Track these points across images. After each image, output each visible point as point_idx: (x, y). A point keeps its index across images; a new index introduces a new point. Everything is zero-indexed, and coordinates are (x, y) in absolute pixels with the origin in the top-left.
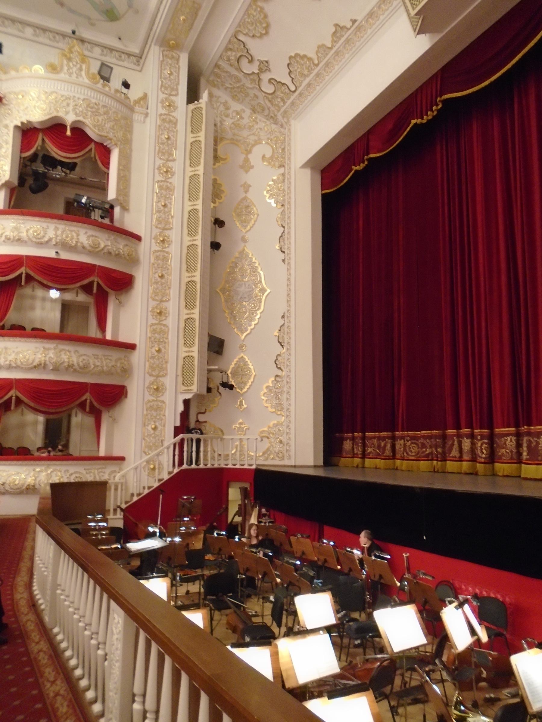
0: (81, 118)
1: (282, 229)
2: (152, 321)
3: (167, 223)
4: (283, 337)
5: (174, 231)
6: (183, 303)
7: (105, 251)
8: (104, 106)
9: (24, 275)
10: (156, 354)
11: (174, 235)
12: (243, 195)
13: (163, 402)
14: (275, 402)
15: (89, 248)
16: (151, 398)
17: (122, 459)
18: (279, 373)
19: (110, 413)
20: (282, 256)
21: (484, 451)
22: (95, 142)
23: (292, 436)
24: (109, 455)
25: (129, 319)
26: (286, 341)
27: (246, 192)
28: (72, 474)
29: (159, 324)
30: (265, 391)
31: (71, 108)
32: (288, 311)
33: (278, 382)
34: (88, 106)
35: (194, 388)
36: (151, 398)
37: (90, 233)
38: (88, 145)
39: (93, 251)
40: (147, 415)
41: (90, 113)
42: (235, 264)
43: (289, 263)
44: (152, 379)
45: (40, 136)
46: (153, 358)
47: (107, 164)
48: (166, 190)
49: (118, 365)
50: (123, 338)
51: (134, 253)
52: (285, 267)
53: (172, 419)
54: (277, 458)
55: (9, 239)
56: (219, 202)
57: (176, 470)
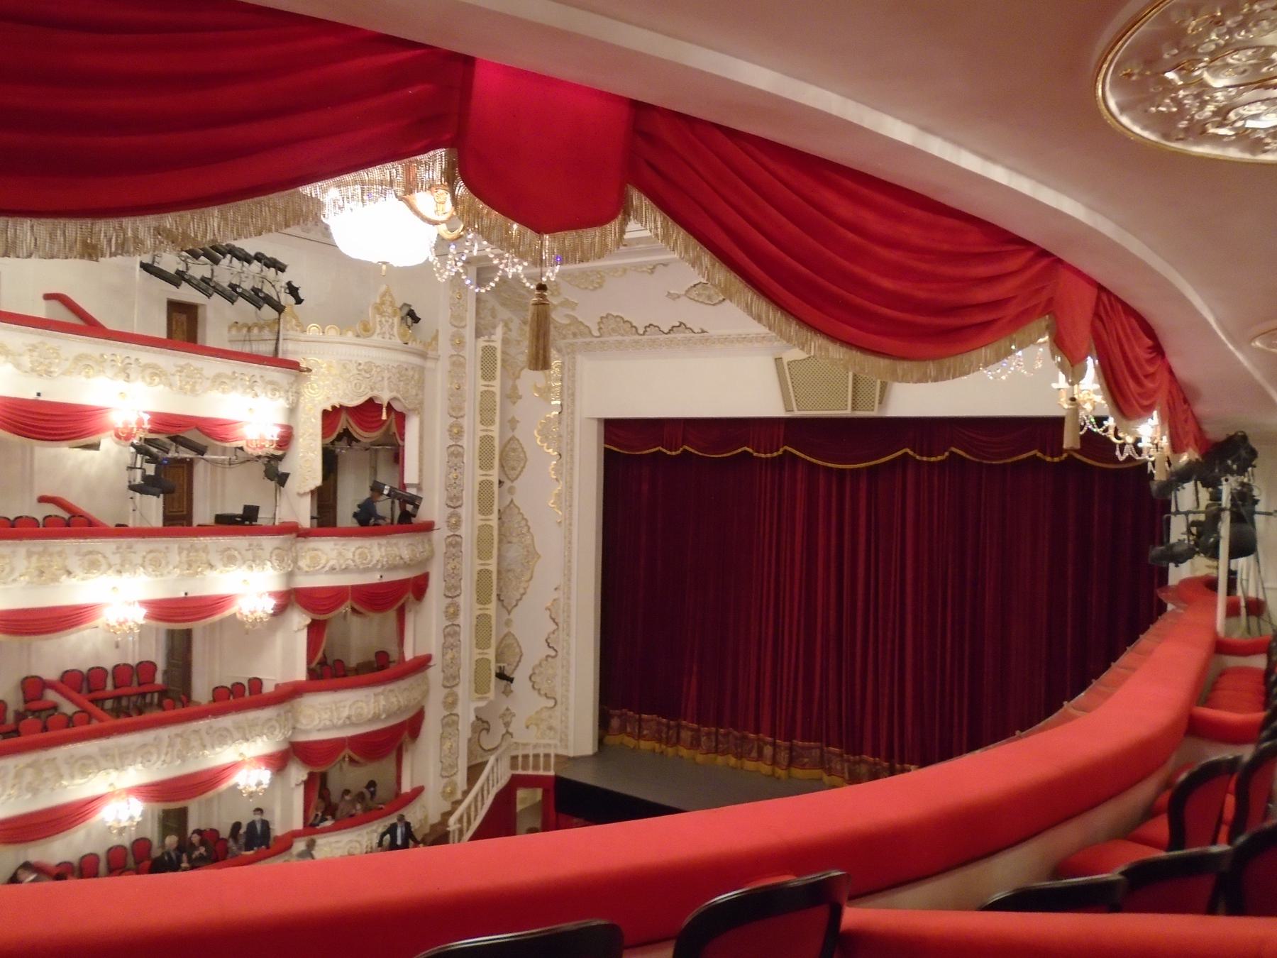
0: (394, 394)
11: (463, 512)
18: (553, 653)
27: (513, 430)
31: (386, 382)
48: (455, 454)
50: (421, 652)
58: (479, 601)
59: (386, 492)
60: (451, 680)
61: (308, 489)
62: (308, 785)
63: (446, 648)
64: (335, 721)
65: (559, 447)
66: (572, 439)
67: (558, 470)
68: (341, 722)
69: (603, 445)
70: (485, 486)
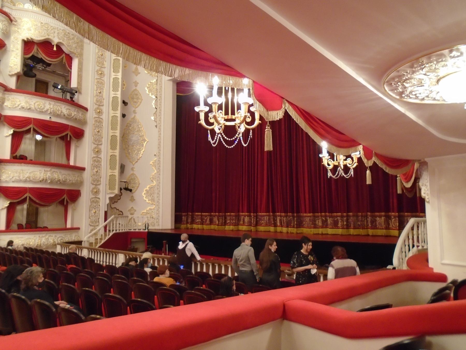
0: (61, 41)
3: (101, 102)
5: (104, 107)
6: (109, 147)
8: (73, 35)
9: (32, 129)
12: (135, 88)
15: (66, 115)
17: (78, 229)
22: (65, 53)
25: (82, 154)
27: (136, 86)
28: (58, 238)
29: (97, 157)
30: (145, 192)
31: (56, 34)
34: (65, 34)
37: (67, 107)
38: (61, 55)
41: (66, 38)
43: (160, 128)
45: (36, 47)
47: (70, 66)
48: (100, 84)
50: (79, 165)
52: (157, 130)
53: (103, 207)
55: (23, 108)
58: (111, 148)
59: (59, 87)
60: (96, 182)
61: (13, 73)
62: (11, 210)
63: (94, 166)
64: (21, 178)
65: (157, 94)
66: (161, 89)
67: (156, 104)
68: (25, 178)
69: (176, 94)
70: (115, 98)
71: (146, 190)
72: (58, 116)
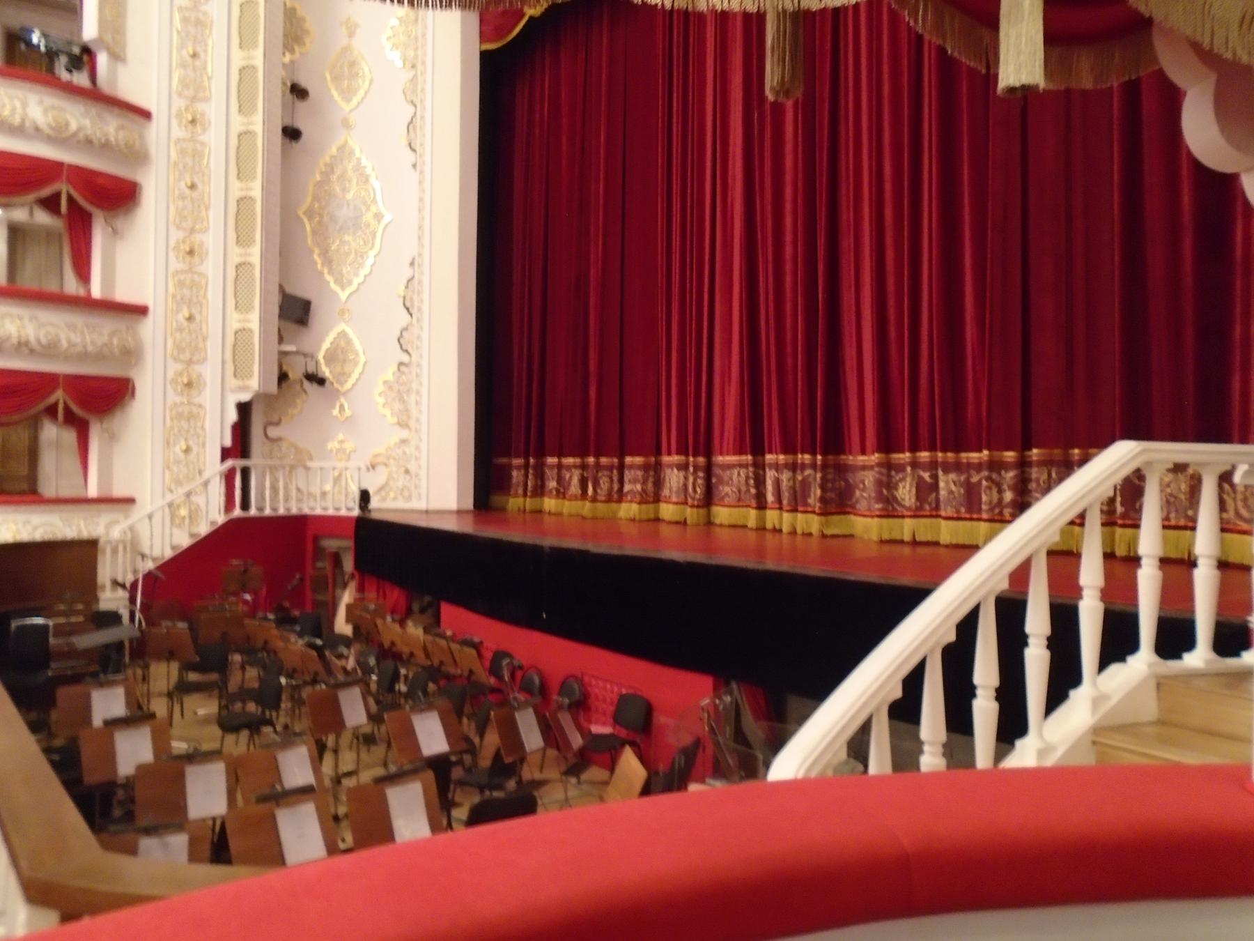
1: (412, 109)
2: (175, 265)
4: (412, 299)
7: (81, 136)
10: (185, 323)
12: (345, 42)
13: (200, 406)
14: (397, 406)
15: (47, 131)
16: (178, 399)
17: (130, 501)
18: (405, 358)
19: (105, 425)
20: (411, 157)
21: (699, 491)
23: (424, 463)
24: (105, 494)
26: (416, 304)
27: (351, 35)
32: (420, 255)
33: (403, 373)
35: (254, 384)
36: (178, 399)
39: (58, 137)
40: (172, 428)
42: (331, 168)
43: (422, 172)
44: (179, 367)
46: (180, 329)
49: (115, 341)
50: (123, 295)
51: (137, 143)
54: (400, 498)
56: (301, 54)
57: (221, 519)
60: (189, 352)
71: (385, 382)
72: (18, 130)
